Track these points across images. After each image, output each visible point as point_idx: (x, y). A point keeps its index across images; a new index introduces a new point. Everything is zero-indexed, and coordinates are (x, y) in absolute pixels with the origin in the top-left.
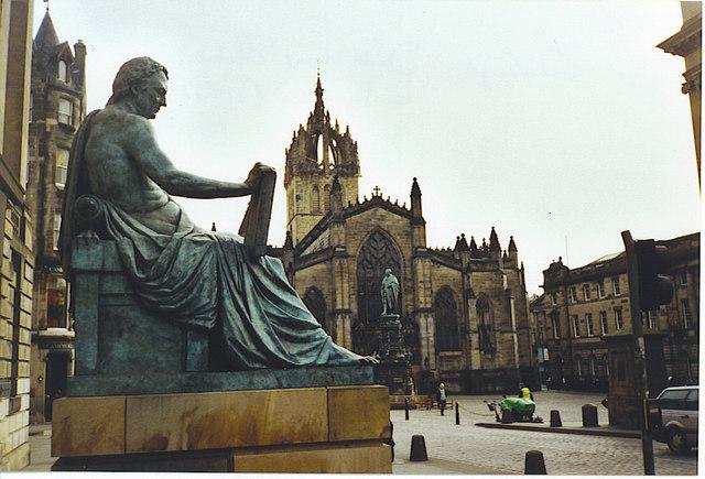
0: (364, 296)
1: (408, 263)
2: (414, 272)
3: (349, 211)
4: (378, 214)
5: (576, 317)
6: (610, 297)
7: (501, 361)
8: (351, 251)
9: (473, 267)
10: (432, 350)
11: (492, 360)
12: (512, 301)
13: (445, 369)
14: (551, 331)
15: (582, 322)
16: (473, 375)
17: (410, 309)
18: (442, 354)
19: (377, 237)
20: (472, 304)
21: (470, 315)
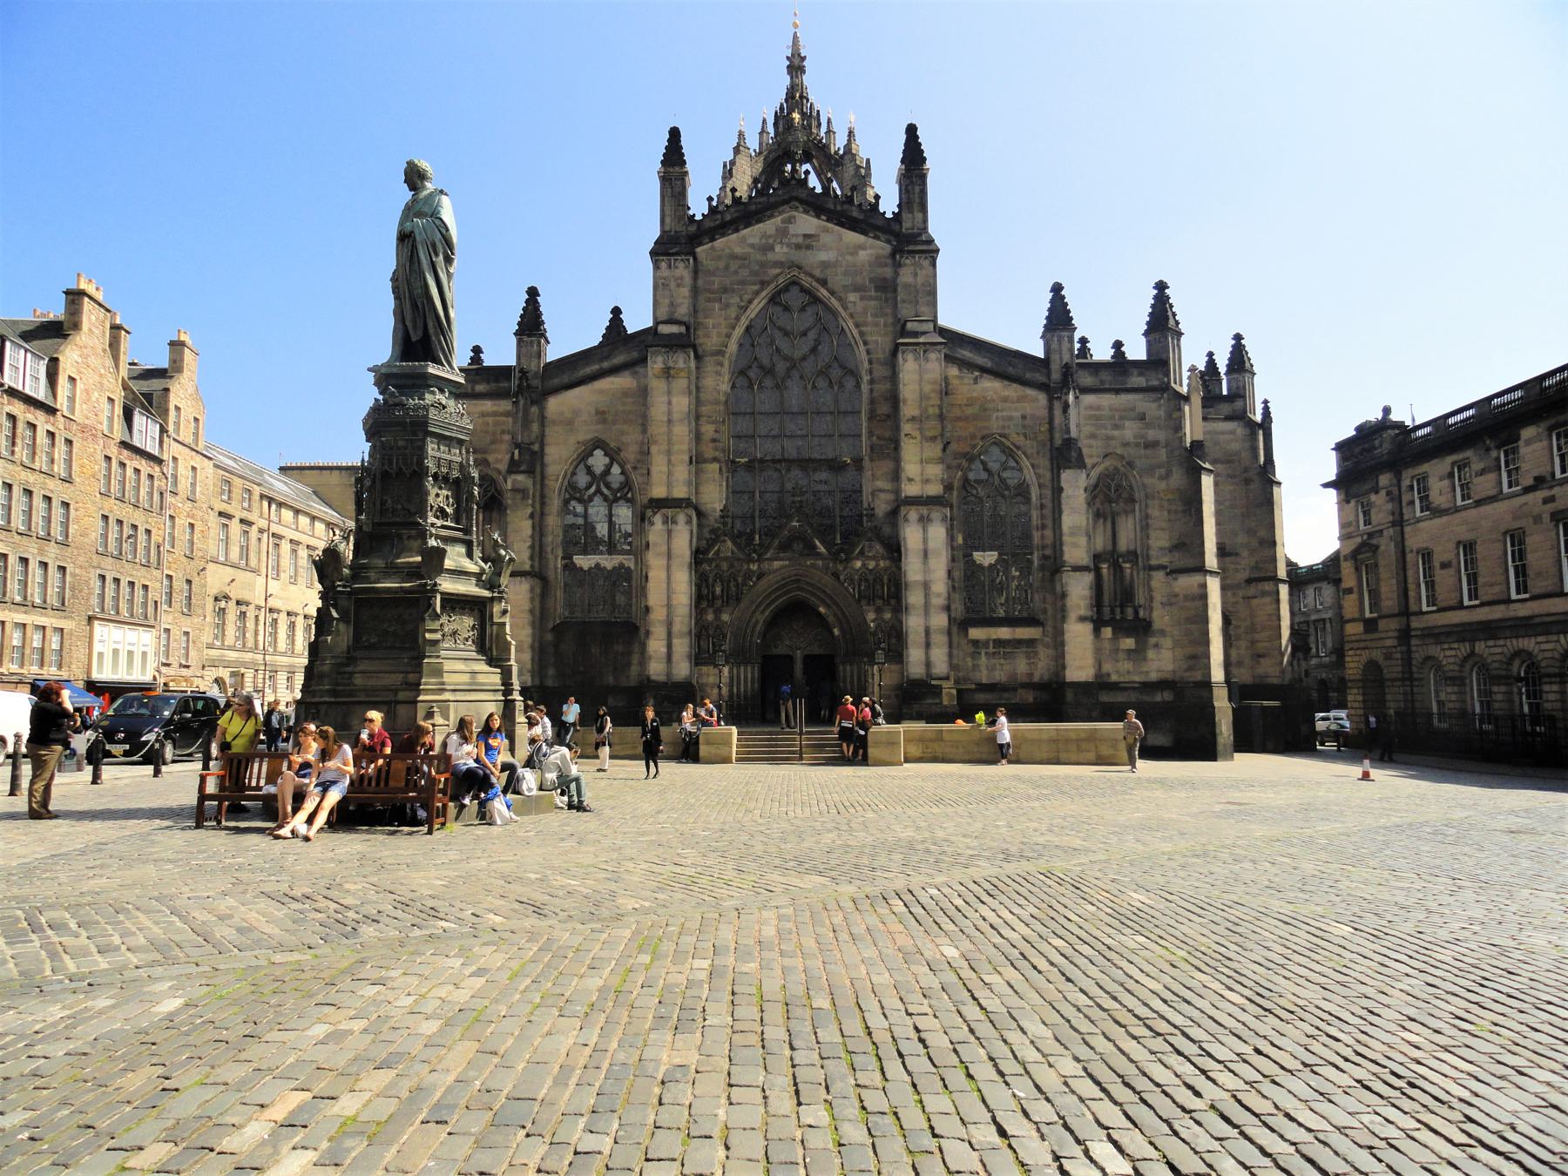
0: (749, 467)
1: (881, 371)
2: (894, 399)
3: (709, 224)
4: (793, 229)
5: (1427, 555)
6: (1539, 482)
7: (1162, 661)
8: (709, 340)
9: (1086, 379)
10: (940, 620)
11: (1137, 654)
12: (1207, 482)
13: (984, 677)
14: (1354, 596)
15: (1444, 566)
16: (1069, 696)
17: (882, 506)
18: (975, 633)
19: (794, 298)
20: (1075, 486)
21: (1067, 521)
